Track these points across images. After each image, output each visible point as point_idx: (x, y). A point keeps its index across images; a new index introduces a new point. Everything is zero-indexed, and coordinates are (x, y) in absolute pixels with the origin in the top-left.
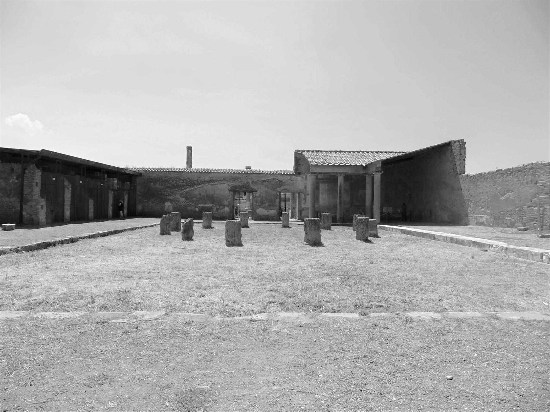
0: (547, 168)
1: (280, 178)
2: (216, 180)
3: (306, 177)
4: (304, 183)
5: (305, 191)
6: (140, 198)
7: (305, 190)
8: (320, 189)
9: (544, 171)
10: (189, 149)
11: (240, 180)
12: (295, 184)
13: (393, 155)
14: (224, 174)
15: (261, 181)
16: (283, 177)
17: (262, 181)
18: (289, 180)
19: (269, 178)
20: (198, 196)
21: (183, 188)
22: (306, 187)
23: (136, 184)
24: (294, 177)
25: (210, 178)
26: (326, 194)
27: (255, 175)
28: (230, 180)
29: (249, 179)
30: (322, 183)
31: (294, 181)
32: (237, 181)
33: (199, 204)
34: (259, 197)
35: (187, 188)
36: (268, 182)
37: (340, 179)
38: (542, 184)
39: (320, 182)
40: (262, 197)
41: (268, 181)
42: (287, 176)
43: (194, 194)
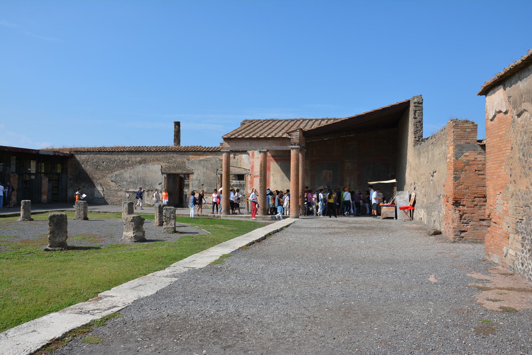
3: (253, 154)
4: (250, 162)
5: (252, 173)
6: (71, 182)
7: (252, 171)
10: (177, 124)
12: (239, 164)
13: (324, 123)
20: (129, 180)
21: (113, 171)
22: (253, 167)
23: (67, 167)
26: (279, 176)
30: (273, 162)
33: (130, 189)
35: (118, 170)
36: (207, 161)
41: (206, 160)
43: (124, 177)
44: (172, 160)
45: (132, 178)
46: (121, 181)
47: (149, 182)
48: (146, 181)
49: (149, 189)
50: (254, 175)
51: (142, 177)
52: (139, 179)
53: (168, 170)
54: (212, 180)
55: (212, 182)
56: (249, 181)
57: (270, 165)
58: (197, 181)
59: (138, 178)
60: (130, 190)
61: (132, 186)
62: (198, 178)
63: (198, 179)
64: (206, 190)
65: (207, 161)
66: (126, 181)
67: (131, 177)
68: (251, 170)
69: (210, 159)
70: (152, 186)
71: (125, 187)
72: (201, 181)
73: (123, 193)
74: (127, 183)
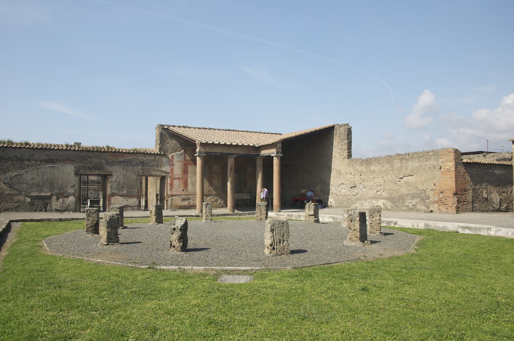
0: (452, 155)
1: (141, 158)
2: (57, 159)
7: (172, 173)
8: (189, 172)
9: (448, 158)
11: (90, 160)
14: (69, 152)
15: (117, 161)
16: (145, 157)
17: (119, 161)
18: (153, 160)
19: (128, 158)
24: (158, 157)
25: (48, 156)
27: (110, 154)
28: (77, 160)
29: (102, 159)
31: (158, 162)
32: (86, 161)
34: (116, 181)
36: (127, 162)
37: (231, 162)
38: (446, 170)
39: (189, 164)
40: (119, 181)
42: (150, 156)
44: (88, 160)
45: (36, 180)
46: (19, 183)
47: (58, 184)
48: (54, 184)
49: (58, 193)
50: (174, 177)
51: (49, 178)
52: (45, 181)
53: (83, 172)
54: (133, 182)
55: (132, 184)
56: (169, 183)
57: (187, 168)
58: (116, 183)
59: (44, 180)
60: (33, 194)
61: (35, 189)
62: (117, 180)
63: (118, 181)
64: (126, 192)
65: (127, 162)
66: (27, 184)
67: (33, 179)
68: (171, 172)
69: (130, 161)
70: (63, 189)
71: (25, 190)
72: (121, 182)
73: (21, 198)
74: (28, 185)
